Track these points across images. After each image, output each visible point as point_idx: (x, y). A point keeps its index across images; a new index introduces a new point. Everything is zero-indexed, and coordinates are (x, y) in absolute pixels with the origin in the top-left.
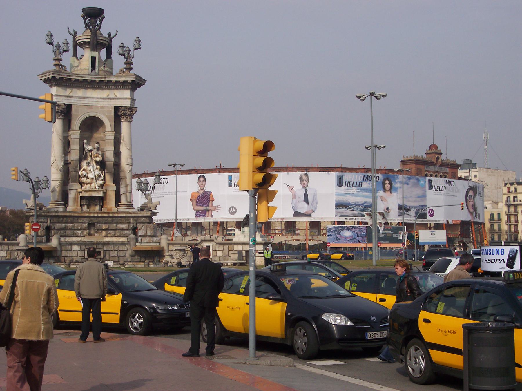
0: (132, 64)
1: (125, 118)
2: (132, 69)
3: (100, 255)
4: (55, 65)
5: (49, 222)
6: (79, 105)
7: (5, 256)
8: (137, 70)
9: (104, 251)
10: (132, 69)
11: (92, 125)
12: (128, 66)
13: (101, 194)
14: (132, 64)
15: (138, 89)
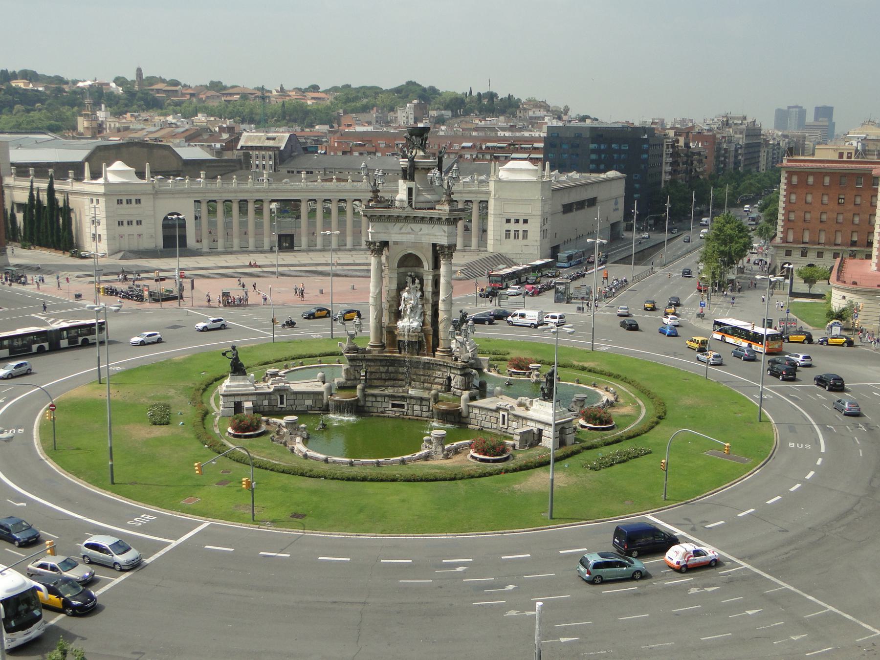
5: (364, 365)
6: (396, 243)
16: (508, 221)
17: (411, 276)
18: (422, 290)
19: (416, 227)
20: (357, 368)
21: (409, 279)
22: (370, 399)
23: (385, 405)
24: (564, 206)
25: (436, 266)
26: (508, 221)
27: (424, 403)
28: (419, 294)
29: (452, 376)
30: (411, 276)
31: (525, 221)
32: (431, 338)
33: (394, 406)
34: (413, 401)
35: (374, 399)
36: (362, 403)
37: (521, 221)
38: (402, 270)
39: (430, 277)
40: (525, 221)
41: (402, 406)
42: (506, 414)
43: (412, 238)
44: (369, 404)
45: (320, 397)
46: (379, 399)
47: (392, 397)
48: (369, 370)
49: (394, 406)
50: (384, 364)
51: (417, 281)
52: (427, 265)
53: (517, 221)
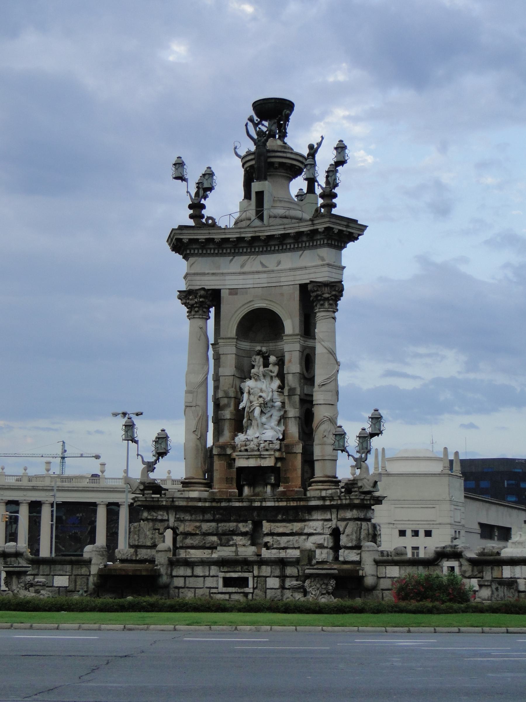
0: (335, 196)
1: (318, 306)
2: (334, 206)
3: (247, 586)
4: (191, 217)
5: (172, 519)
6: (233, 292)
7: (67, 584)
8: (343, 207)
9: (254, 577)
10: (334, 206)
11: (261, 324)
12: (328, 201)
13: (269, 462)
14: (335, 196)
15: (350, 245)
16: (402, 533)
17: (259, 353)
18: (281, 376)
19: (270, 260)
20: (159, 525)
21: (258, 360)
22: (181, 571)
23: (210, 582)
24: (482, 525)
25: (308, 329)
26: (402, 533)
27: (290, 571)
28: (277, 383)
29: (341, 525)
30: (259, 353)
31: (428, 533)
32: (298, 461)
33: (228, 582)
34: (266, 570)
35: (189, 572)
36: (165, 579)
37: (422, 533)
38: (245, 345)
39: (297, 347)
40: (428, 533)
41: (244, 582)
42: (455, 563)
43: (263, 280)
44: (179, 582)
45: (84, 571)
46: (199, 571)
47: (222, 563)
48: (181, 529)
49: (228, 582)
50: (208, 516)
51: (272, 359)
52: (291, 325)
53: (416, 533)
